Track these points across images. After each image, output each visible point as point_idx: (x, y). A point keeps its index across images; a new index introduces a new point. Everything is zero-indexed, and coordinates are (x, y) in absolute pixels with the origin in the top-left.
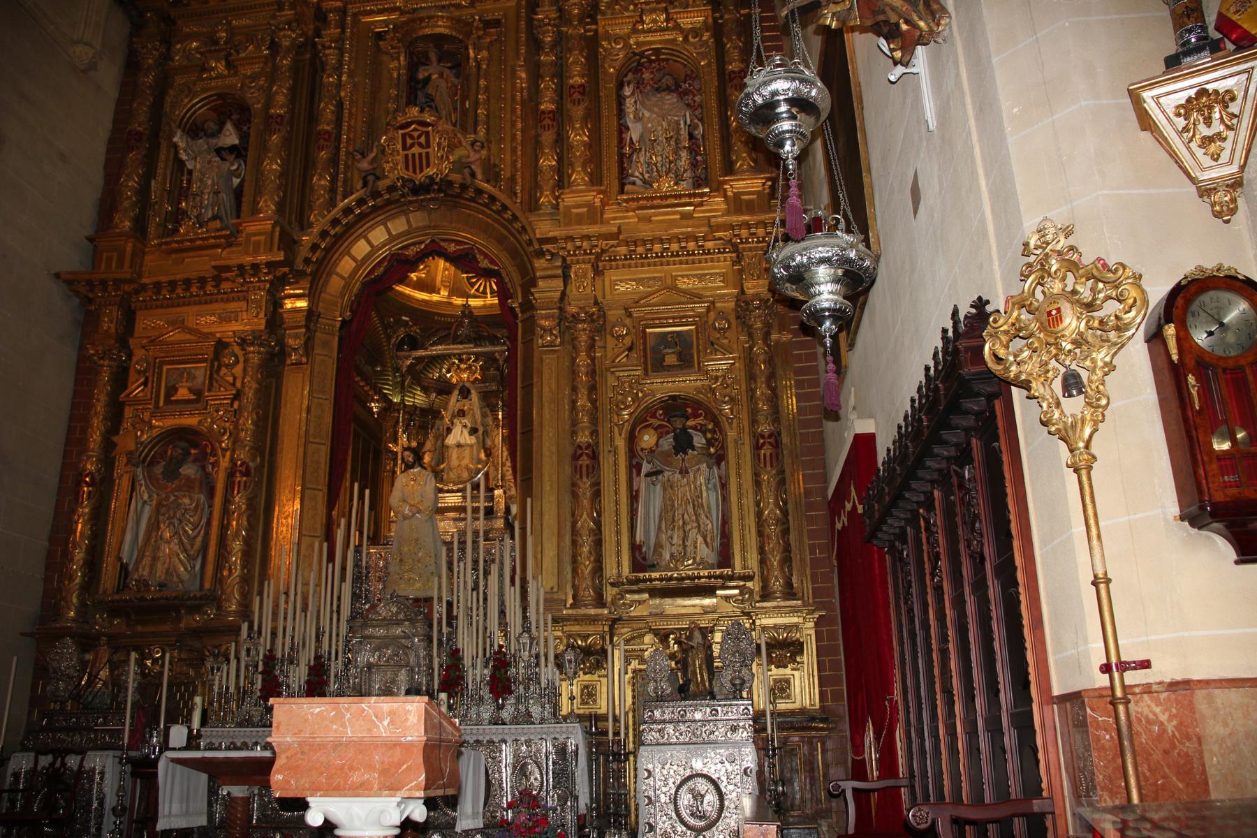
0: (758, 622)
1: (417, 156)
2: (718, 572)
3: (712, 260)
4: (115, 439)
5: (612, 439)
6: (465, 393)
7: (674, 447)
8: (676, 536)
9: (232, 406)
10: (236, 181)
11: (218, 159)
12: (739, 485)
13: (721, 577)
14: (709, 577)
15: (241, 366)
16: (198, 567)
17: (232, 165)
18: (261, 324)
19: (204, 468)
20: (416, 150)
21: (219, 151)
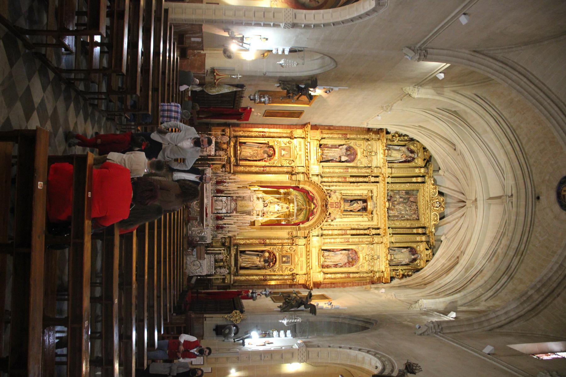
6: (288, 208)
10: (335, 159)
21: (340, 157)
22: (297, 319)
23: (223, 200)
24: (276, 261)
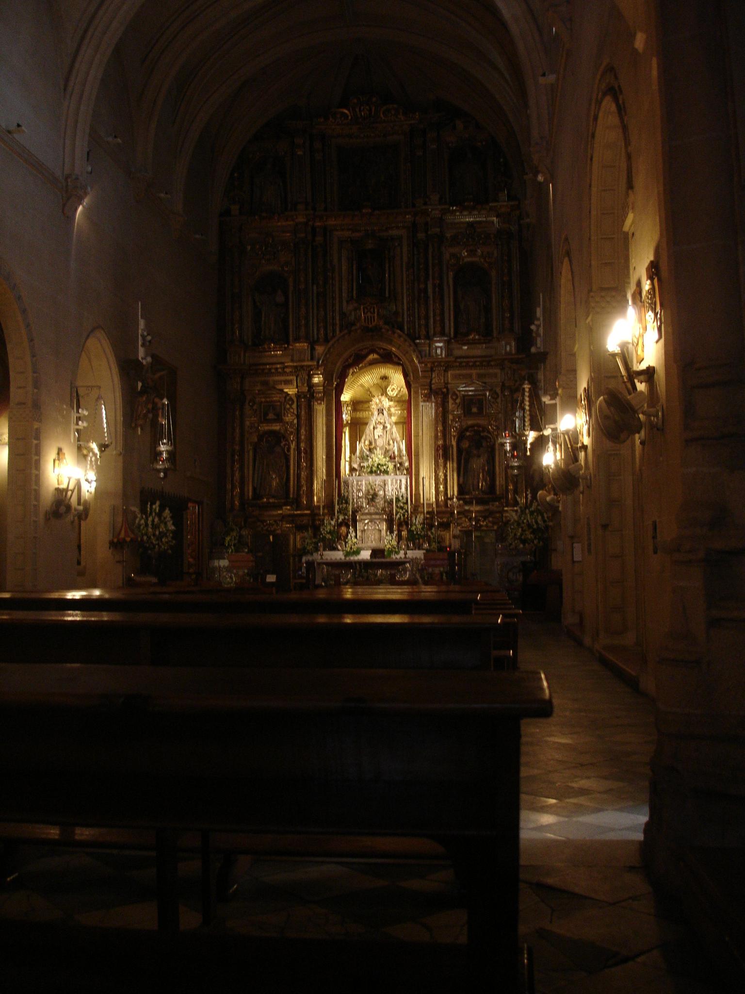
0: (504, 515)
20: (369, 314)
22: (524, 389)
23: (362, 528)
24: (479, 426)
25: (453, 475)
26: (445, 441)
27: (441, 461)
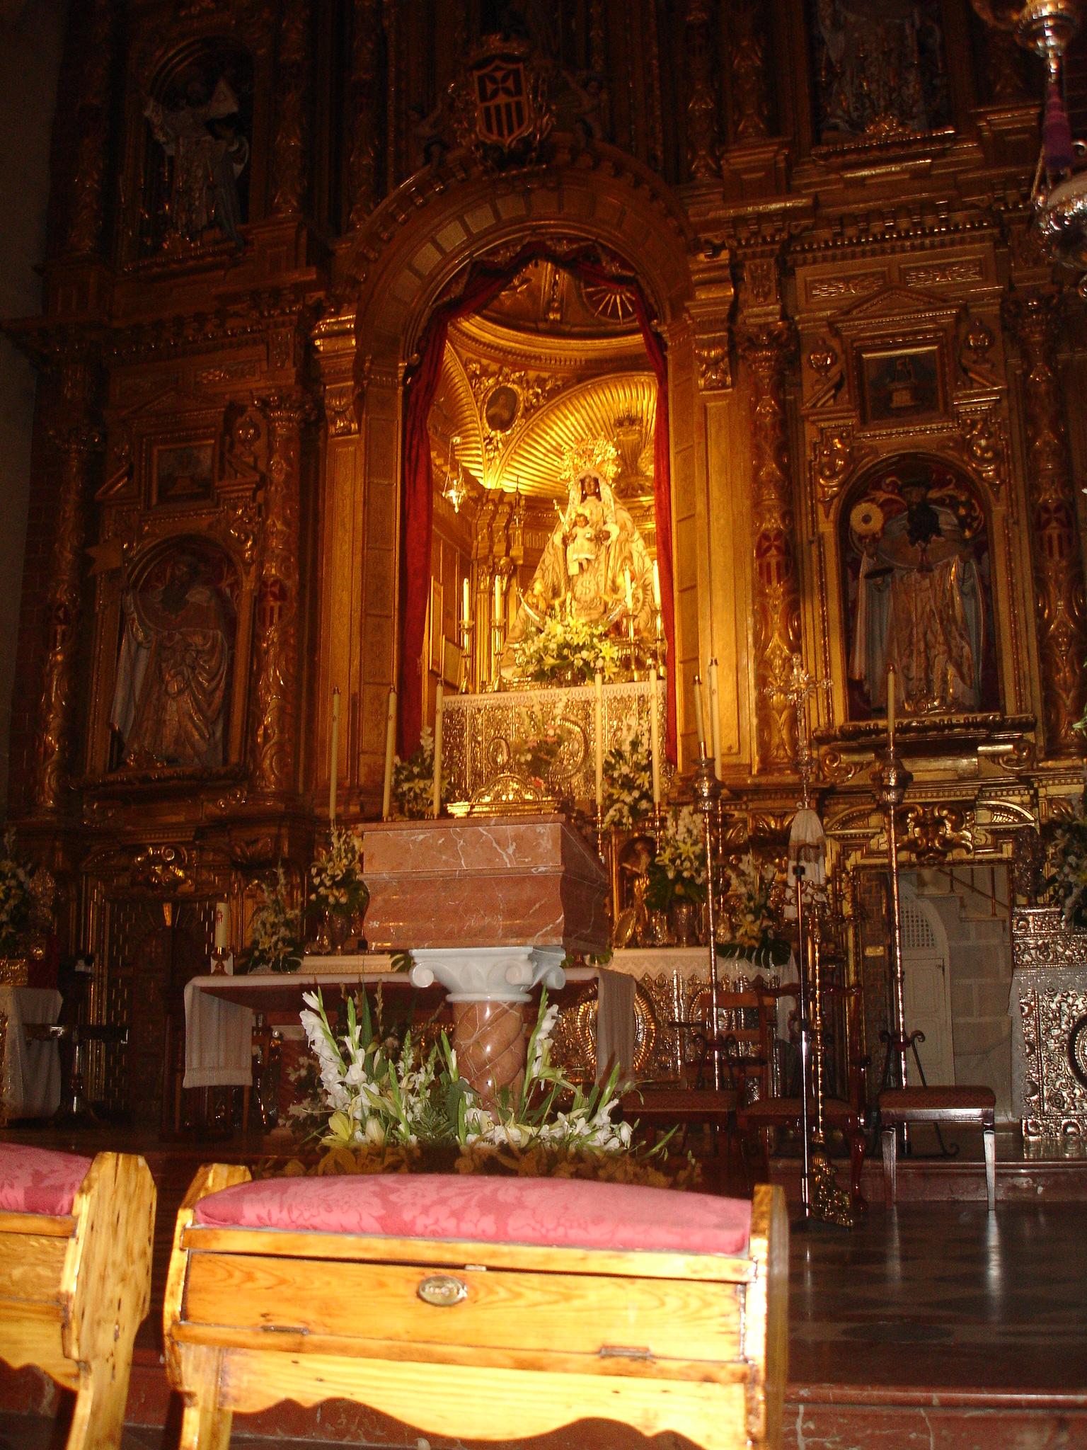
0: (1042, 792)
1: (503, 110)
2: (979, 717)
3: (962, 242)
4: (92, 552)
5: (815, 523)
7: (910, 533)
8: (914, 665)
9: (254, 500)
10: (238, 168)
11: (209, 138)
12: (1012, 586)
13: (984, 724)
14: (967, 725)
15: (263, 439)
16: (218, 734)
17: (231, 144)
18: (290, 375)
19: (219, 593)
20: (502, 99)
21: (211, 126)
25: (826, 649)
26: (789, 514)
27: (777, 589)
